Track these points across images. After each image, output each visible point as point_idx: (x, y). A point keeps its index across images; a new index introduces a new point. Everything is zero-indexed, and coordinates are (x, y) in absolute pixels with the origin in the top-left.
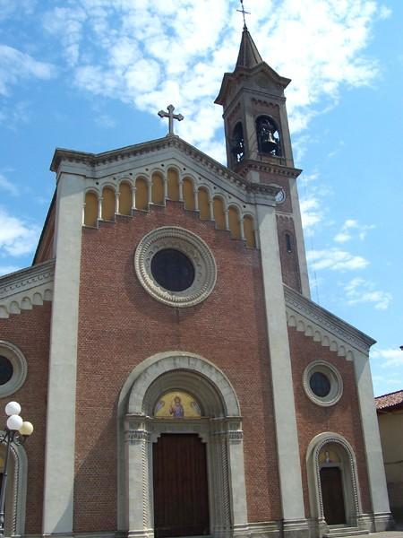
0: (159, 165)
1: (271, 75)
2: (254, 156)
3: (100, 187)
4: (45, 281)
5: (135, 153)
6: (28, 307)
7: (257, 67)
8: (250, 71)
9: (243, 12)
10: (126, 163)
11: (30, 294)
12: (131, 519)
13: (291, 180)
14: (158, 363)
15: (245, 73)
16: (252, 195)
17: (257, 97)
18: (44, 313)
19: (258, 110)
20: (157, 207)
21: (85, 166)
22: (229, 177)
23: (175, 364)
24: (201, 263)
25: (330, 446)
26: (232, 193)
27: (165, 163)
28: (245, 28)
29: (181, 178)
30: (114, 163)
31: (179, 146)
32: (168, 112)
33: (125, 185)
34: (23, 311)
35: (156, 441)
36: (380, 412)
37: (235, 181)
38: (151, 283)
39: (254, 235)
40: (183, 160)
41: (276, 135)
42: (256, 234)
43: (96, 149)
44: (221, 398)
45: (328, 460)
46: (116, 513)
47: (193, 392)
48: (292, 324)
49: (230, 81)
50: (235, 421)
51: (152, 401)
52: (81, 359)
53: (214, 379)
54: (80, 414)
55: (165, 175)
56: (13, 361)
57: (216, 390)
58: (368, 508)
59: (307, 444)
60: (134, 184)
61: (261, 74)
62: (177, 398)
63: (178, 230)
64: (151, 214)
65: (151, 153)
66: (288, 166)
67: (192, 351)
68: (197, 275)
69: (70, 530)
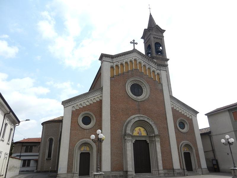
1: (160, 29)
3: (114, 65)
4: (101, 93)
5: (124, 55)
6: (95, 101)
8: (153, 28)
11: (95, 97)
12: (128, 167)
14: (135, 118)
16: (159, 67)
17: (155, 36)
18: (100, 103)
20: (132, 71)
21: (110, 59)
22: (152, 62)
23: (139, 118)
24: (145, 88)
25: (187, 145)
27: (133, 58)
28: (150, 14)
29: (138, 62)
30: (118, 58)
31: (137, 52)
32: (133, 42)
33: (122, 64)
34: (94, 103)
35: (134, 142)
36: (202, 135)
37: (154, 63)
40: (138, 57)
41: (161, 48)
42: (161, 79)
43: (113, 53)
44: (153, 129)
45: (185, 150)
46: (123, 165)
47: (144, 127)
49: (146, 31)
50: (158, 136)
53: (151, 123)
54: (112, 134)
56: (91, 118)
57: (151, 126)
58: (200, 166)
59: (179, 144)
60: (124, 64)
62: (140, 129)
64: (130, 73)
65: (129, 55)
68: (144, 92)
69: (110, 170)
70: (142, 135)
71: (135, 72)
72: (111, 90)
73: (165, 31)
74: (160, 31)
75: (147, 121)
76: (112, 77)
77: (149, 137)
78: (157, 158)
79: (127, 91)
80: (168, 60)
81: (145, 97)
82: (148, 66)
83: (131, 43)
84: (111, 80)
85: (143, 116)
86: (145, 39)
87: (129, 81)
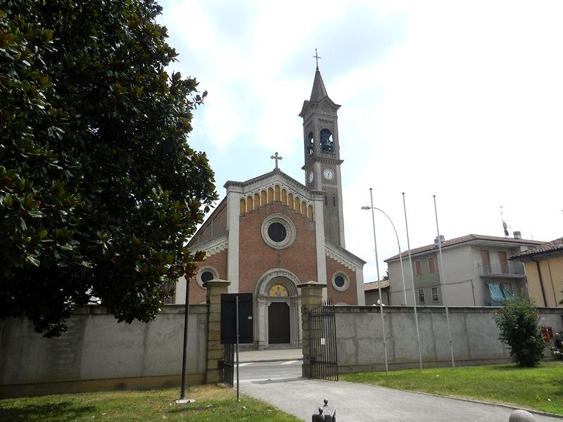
2: (318, 154)
8: (318, 102)
10: (256, 185)
14: (272, 273)
15: (316, 103)
17: (321, 118)
18: (226, 252)
20: (272, 203)
26: (304, 197)
28: (317, 69)
32: (275, 156)
33: (257, 194)
36: (366, 292)
38: (268, 238)
39: (312, 214)
41: (331, 139)
48: (328, 255)
51: (268, 289)
52: (240, 274)
53: (293, 280)
55: (274, 189)
56: (213, 274)
61: (325, 103)
66: (337, 159)
67: (285, 268)
70: (282, 295)
71: (276, 206)
72: (241, 234)
73: (340, 106)
76: (243, 215)
77: (291, 298)
78: (298, 325)
79: (263, 235)
81: (288, 242)
83: (272, 157)
86: (306, 119)
87: (264, 222)
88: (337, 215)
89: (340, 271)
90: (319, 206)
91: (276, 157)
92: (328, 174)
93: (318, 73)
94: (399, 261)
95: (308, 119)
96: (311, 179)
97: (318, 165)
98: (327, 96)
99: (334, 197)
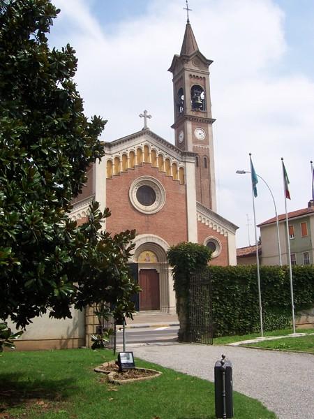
0: (140, 145)
2: (189, 112)
3: (113, 158)
5: (129, 140)
7: (193, 54)
8: (189, 57)
9: (187, 9)
13: (209, 125)
16: (184, 157)
17: (193, 74)
19: (193, 81)
20: (140, 165)
26: (174, 158)
28: (188, 21)
36: (238, 258)
39: (183, 176)
48: (199, 219)
53: (163, 246)
61: (196, 58)
63: (149, 177)
64: (137, 169)
67: (154, 234)
73: (212, 61)
74: (202, 61)
75: (158, 243)
76: (109, 179)
77: (161, 265)
80: (212, 121)
82: (166, 156)
84: (107, 183)
85: (154, 236)
86: (176, 74)
88: (209, 178)
89: (212, 237)
90: (190, 168)
91: (145, 116)
92: (199, 134)
93: (188, 26)
94: (276, 225)
95: (179, 74)
96: (181, 140)
97: (189, 125)
98: (198, 52)
99: (205, 159)
